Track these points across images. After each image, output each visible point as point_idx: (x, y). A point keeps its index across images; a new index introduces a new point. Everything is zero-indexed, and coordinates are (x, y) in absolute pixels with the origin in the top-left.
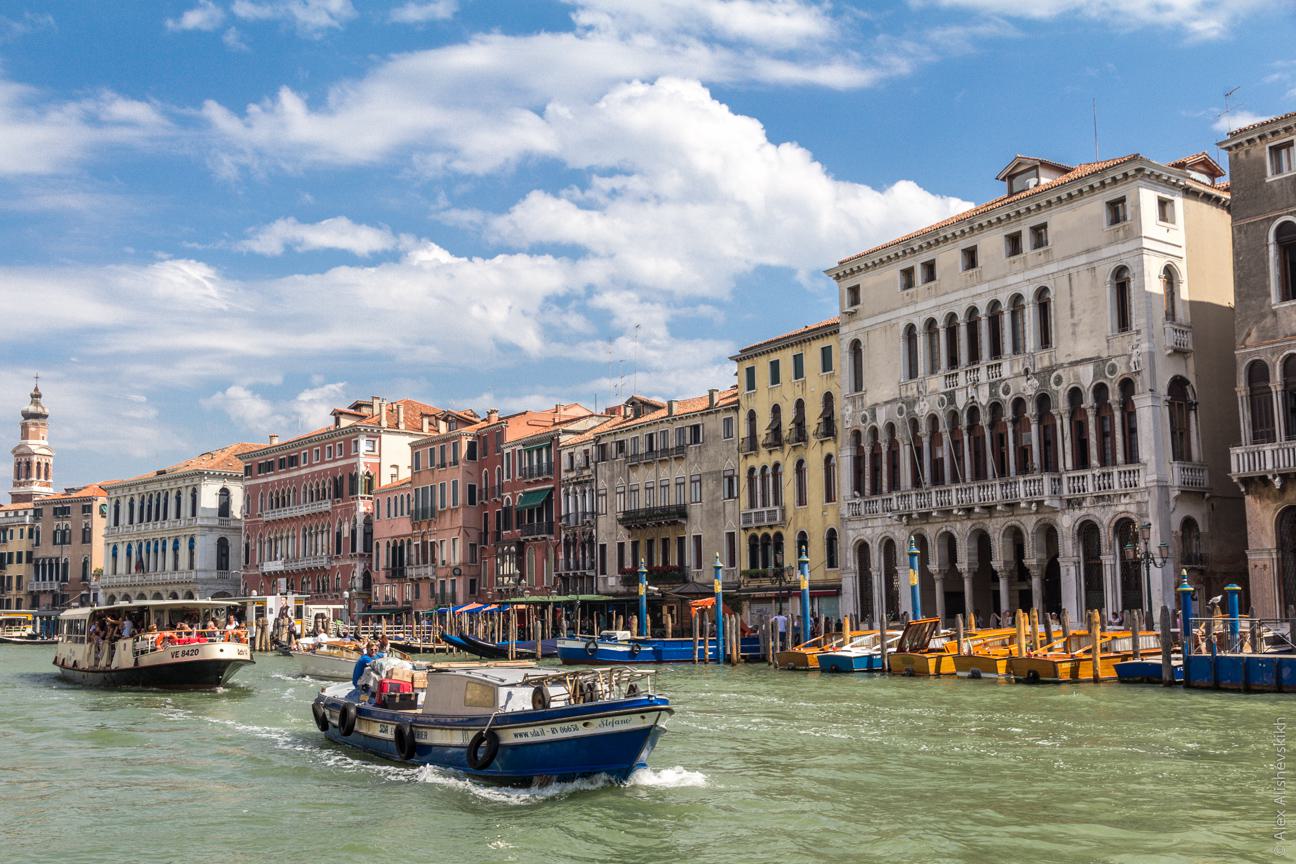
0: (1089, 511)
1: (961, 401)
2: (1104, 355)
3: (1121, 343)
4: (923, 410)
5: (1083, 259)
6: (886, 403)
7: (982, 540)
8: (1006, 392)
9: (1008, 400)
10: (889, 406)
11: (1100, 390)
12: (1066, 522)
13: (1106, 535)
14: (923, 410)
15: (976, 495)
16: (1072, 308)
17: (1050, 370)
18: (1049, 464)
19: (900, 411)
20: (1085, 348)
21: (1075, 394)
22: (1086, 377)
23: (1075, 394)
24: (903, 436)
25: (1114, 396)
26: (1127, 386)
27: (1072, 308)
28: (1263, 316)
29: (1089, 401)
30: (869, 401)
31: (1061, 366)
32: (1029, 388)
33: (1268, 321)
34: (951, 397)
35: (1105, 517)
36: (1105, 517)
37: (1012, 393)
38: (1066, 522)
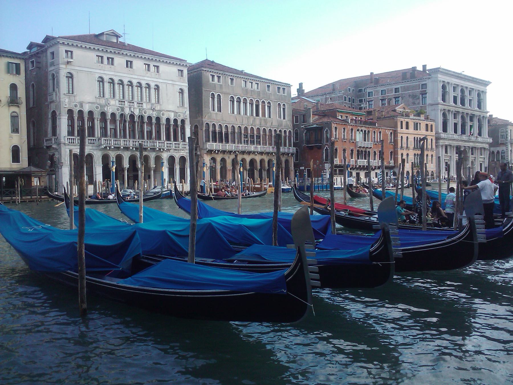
0: (172, 153)
1: (127, 112)
2: (177, 111)
3: (181, 110)
4: (109, 111)
5: (171, 82)
6: (90, 103)
7: (119, 158)
8: (145, 113)
9: (146, 116)
10: (90, 104)
11: (175, 121)
12: (165, 156)
13: (177, 161)
14: (109, 111)
15: (122, 143)
16: (167, 94)
17: (160, 111)
18: (159, 137)
19: (97, 107)
20: (171, 107)
21: (168, 120)
22: (172, 117)
23: (168, 120)
24: (97, 116)
25: (179, 123)
26: (183, 121)
27: (167, 94)
28: (209, 113)
29: (172, 123)
30: (79, 99)
31: (164, 110)
32: (154, 115)
33: (210, 114)
34: (123, 109)
35: (177, 156)
36: (177, 156)
37: (147, 114)
38: (165, 156)
